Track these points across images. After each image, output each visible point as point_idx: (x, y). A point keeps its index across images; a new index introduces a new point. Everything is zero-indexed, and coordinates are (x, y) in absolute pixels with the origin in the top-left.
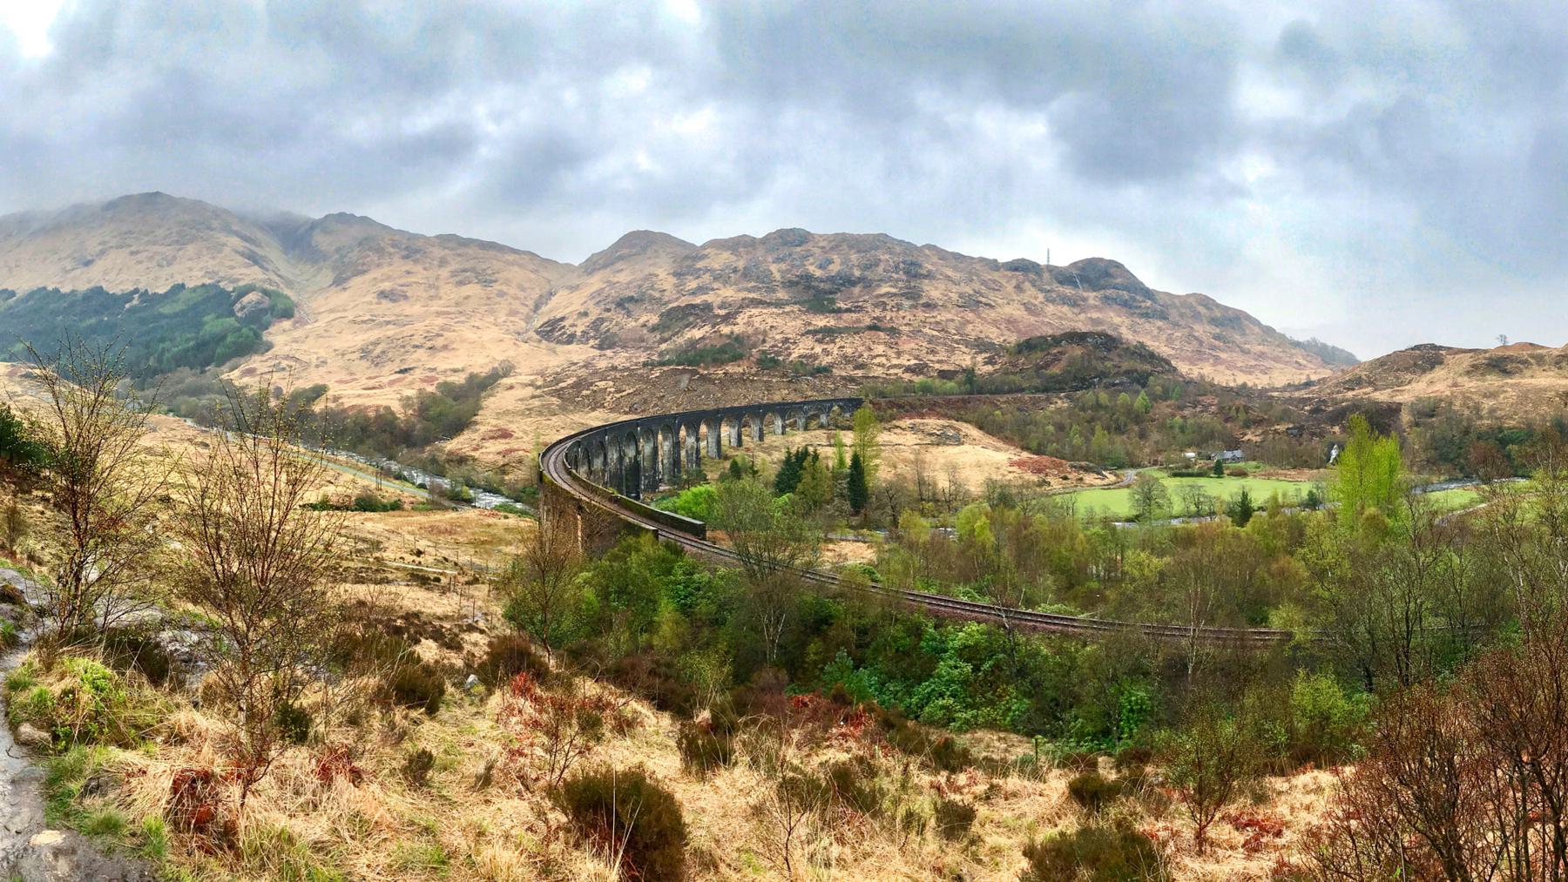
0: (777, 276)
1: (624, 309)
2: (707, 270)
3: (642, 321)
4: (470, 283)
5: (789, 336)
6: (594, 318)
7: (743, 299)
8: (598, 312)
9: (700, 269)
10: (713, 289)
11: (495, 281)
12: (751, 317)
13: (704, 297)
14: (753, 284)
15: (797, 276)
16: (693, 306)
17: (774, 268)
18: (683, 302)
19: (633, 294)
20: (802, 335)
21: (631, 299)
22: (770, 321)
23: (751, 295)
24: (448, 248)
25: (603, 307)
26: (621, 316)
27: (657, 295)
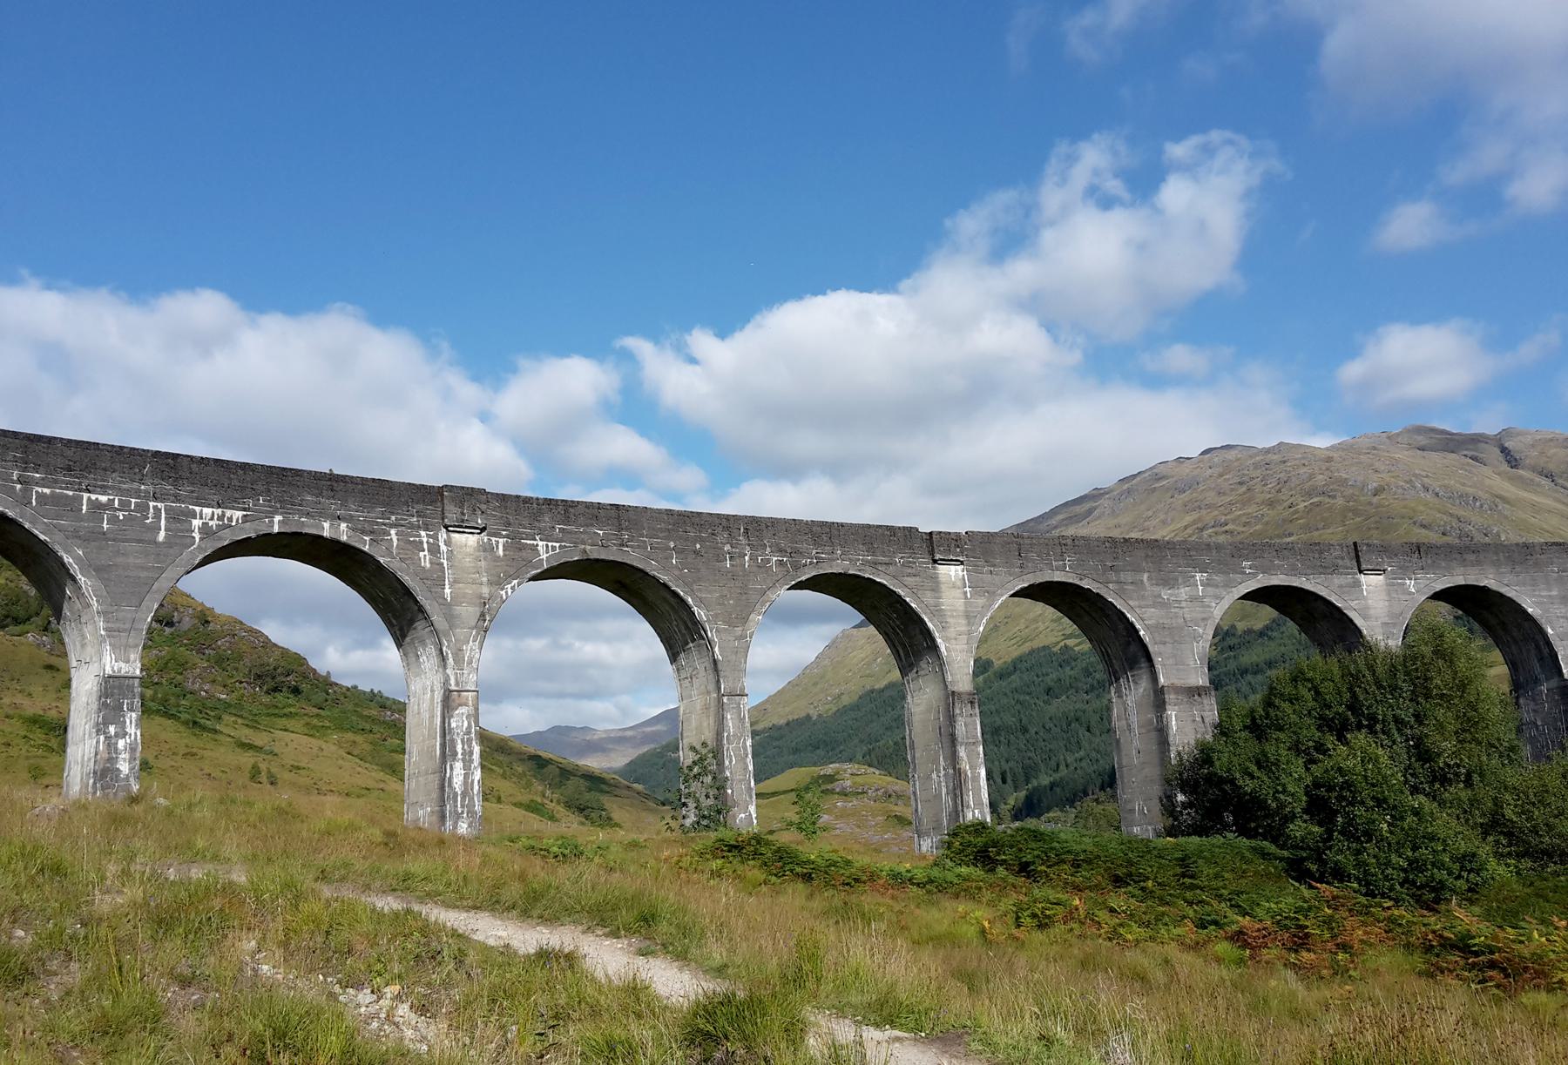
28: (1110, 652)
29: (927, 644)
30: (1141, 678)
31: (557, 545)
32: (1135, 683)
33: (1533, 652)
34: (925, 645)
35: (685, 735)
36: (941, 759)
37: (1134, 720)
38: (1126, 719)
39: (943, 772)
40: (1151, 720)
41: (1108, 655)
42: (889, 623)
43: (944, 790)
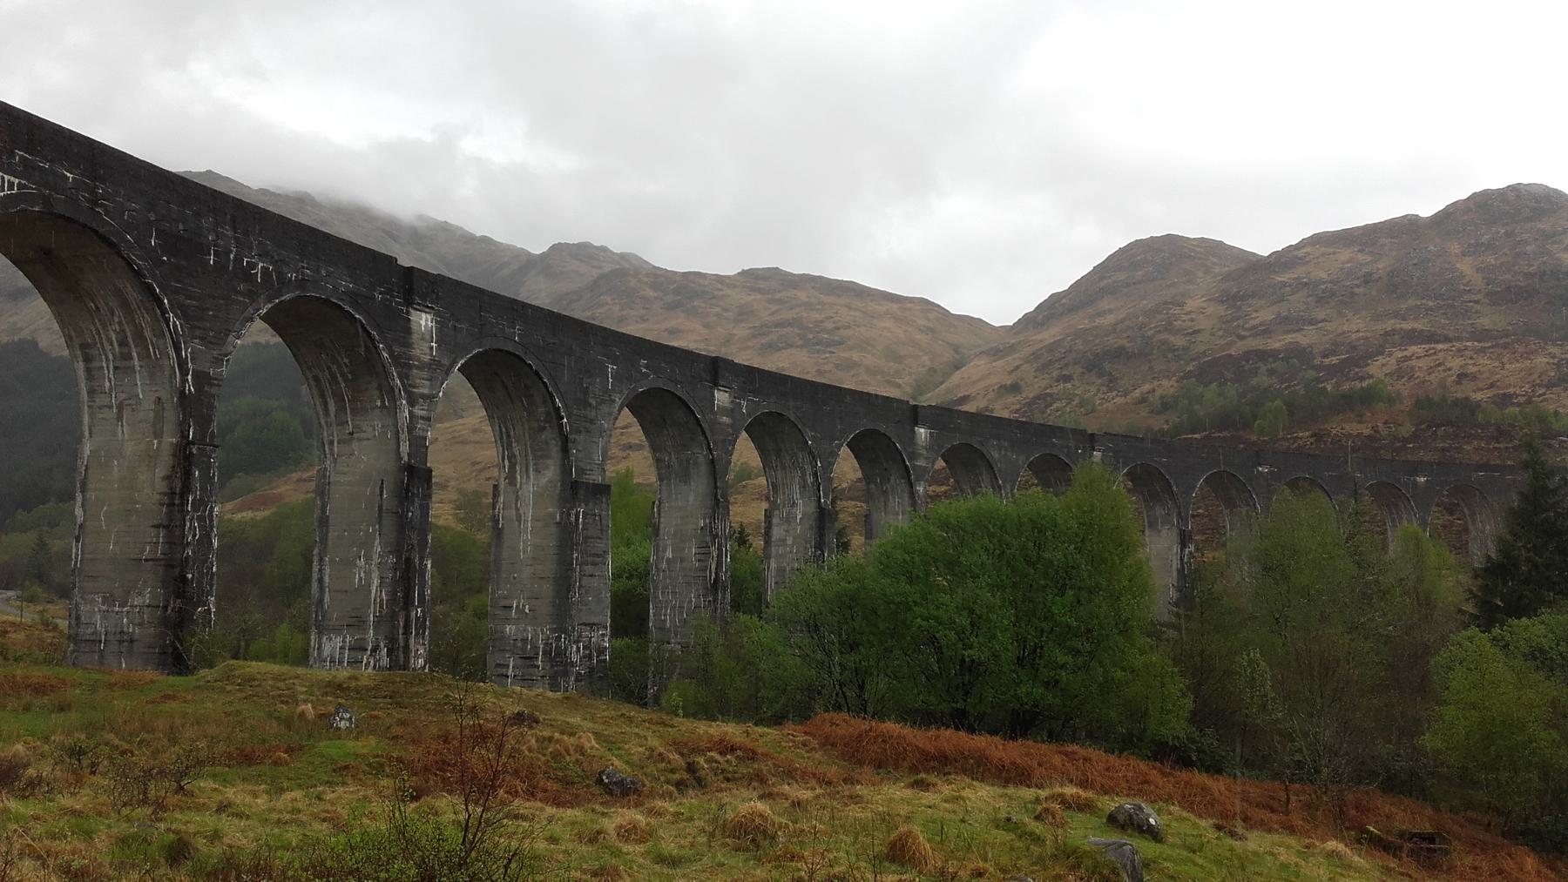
0: (1478, 280)
1: (1101, 375)
2: (1301, 285)
3: (1137, 394)
4: (790, 346)
5: (1512, 390)
6: (1031, 395)
7: (1387, 333)
8: (1043, 384)
9: (1284, 284)
10: (1313, 322)
11: (841, 343)
12: (1407, 359)
13: (1290, 338)
14: (1412, 302)
15: (1532, 275)
16: (1263, 355)
17: (1466, 267)
18: (1237, 349)
19: (1125, 342)
20: (1549, 386)
21: (1119, 354)
22: (1455, 364)
23: (1407, 326)
24: (759, 290)
25: (1055, 374)
26: (1093, 389)
27: (1179, 341)
28: (512, 433)
29: (383, 402)
30: (547, 468)
31: (17, 181)
32: (537, 471)
33: (797, 479)
34: (379, 404)
35: (90, 486)
36: (377, 542)
37: (529, 513)
38: (517, 509)
39: (376, 559)
40: (553, 516)
41: (509, 436)
42: (329, 368)
43: (376, 582)
